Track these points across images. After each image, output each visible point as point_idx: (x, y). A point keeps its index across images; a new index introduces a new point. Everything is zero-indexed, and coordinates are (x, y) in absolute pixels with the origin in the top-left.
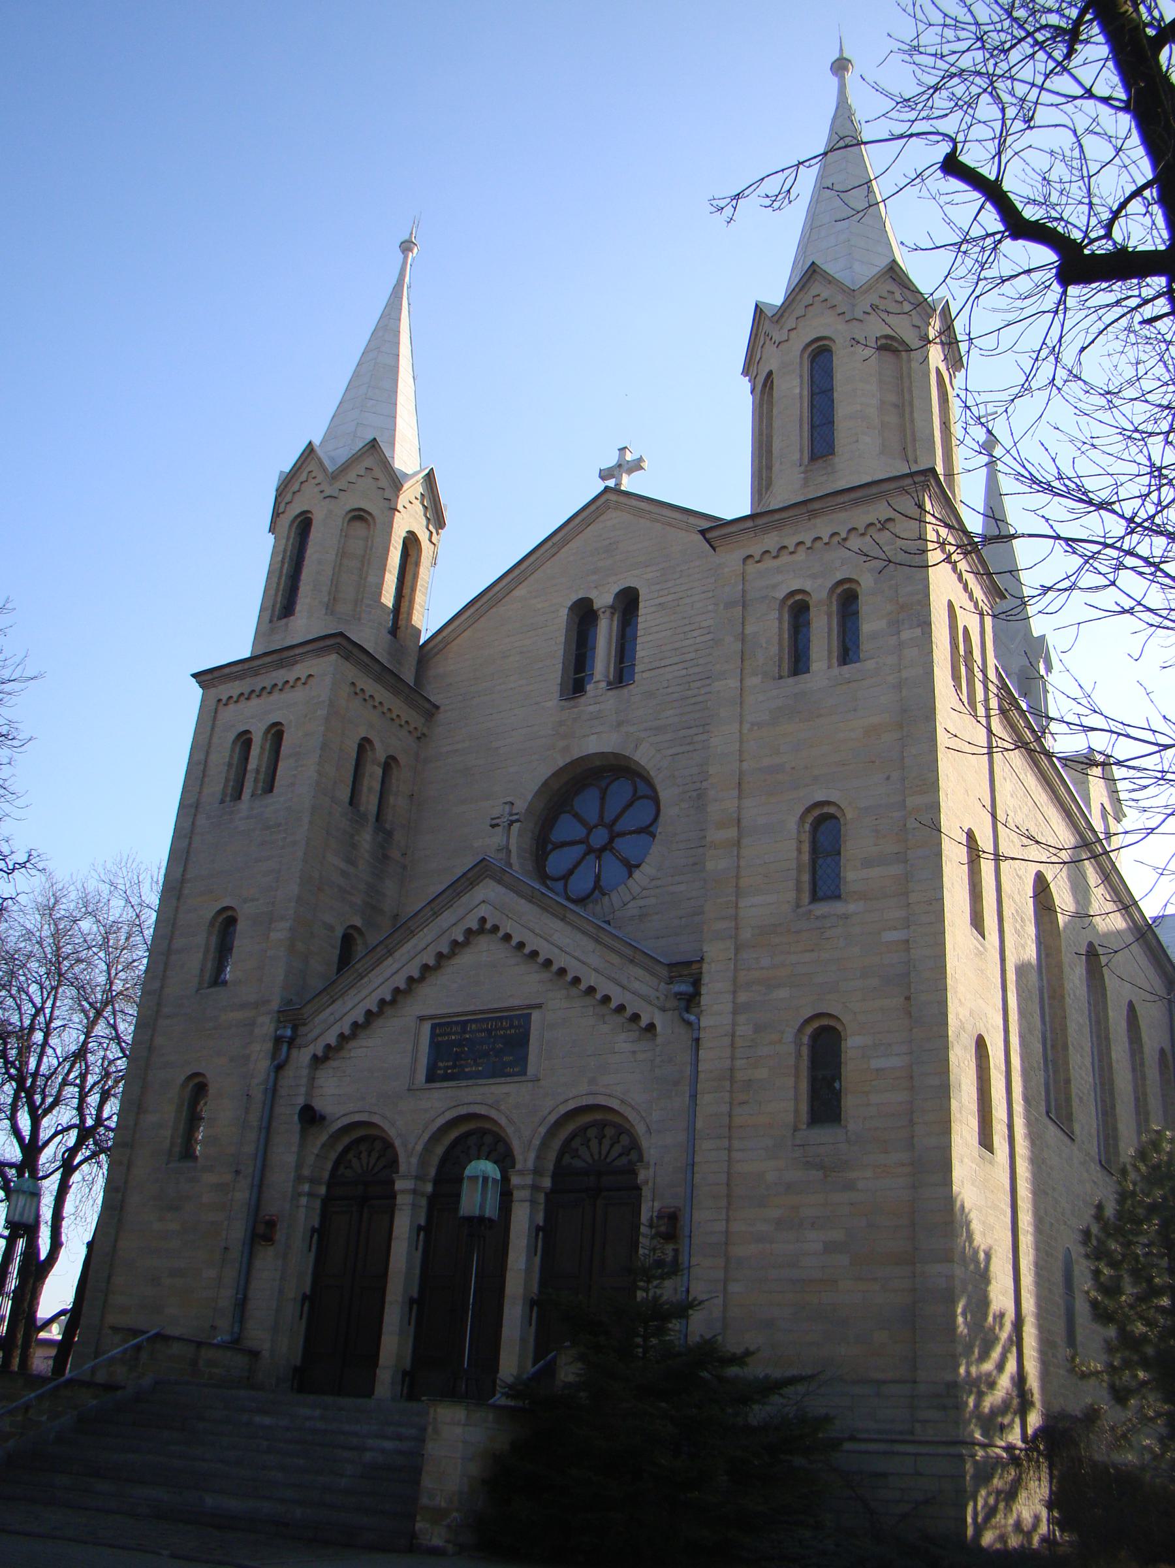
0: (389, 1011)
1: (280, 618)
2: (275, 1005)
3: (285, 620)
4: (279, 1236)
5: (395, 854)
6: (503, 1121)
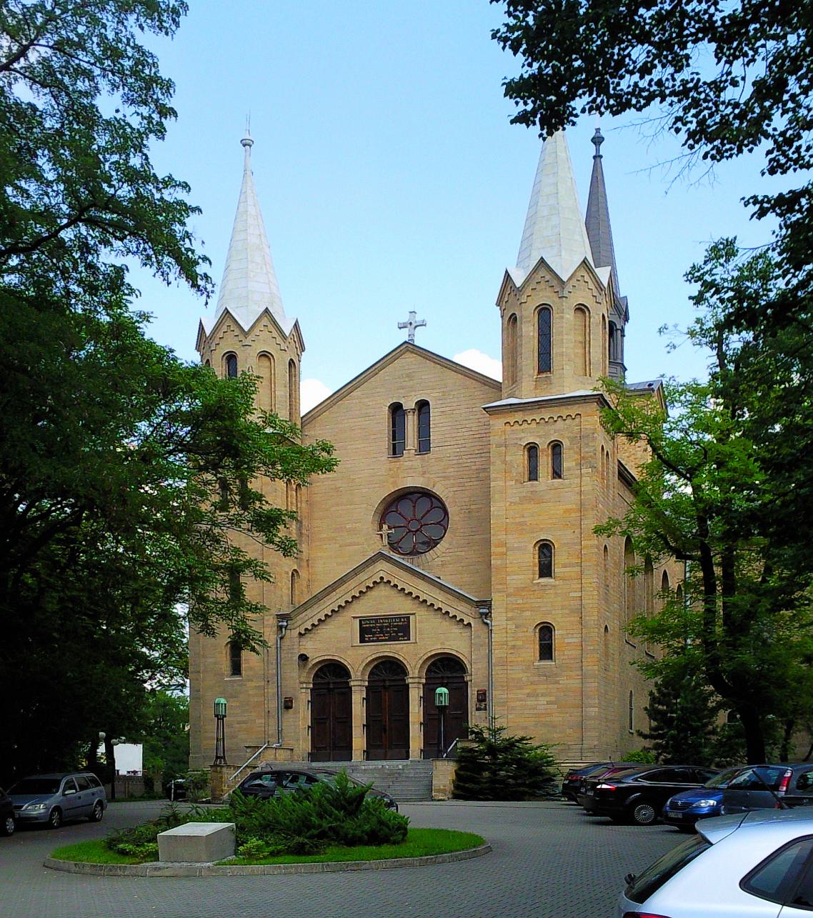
5: (304, 531)
6: (401, 659)
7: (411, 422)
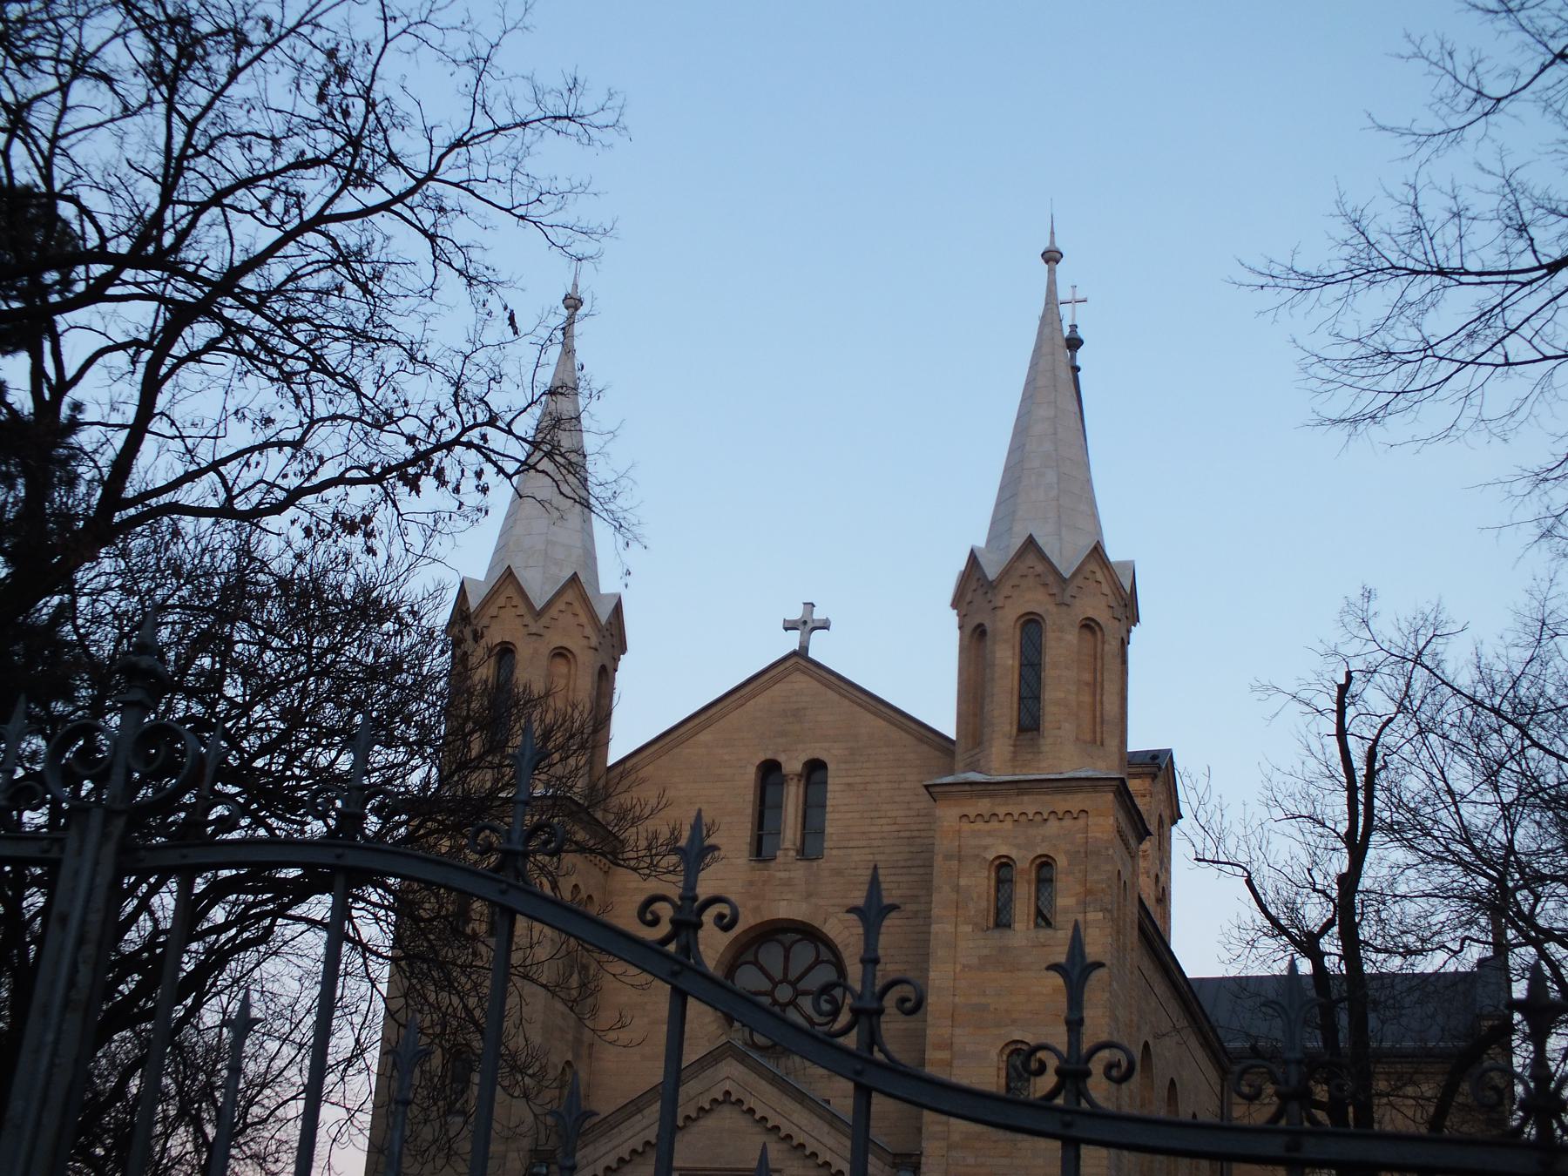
7: (793, 796)
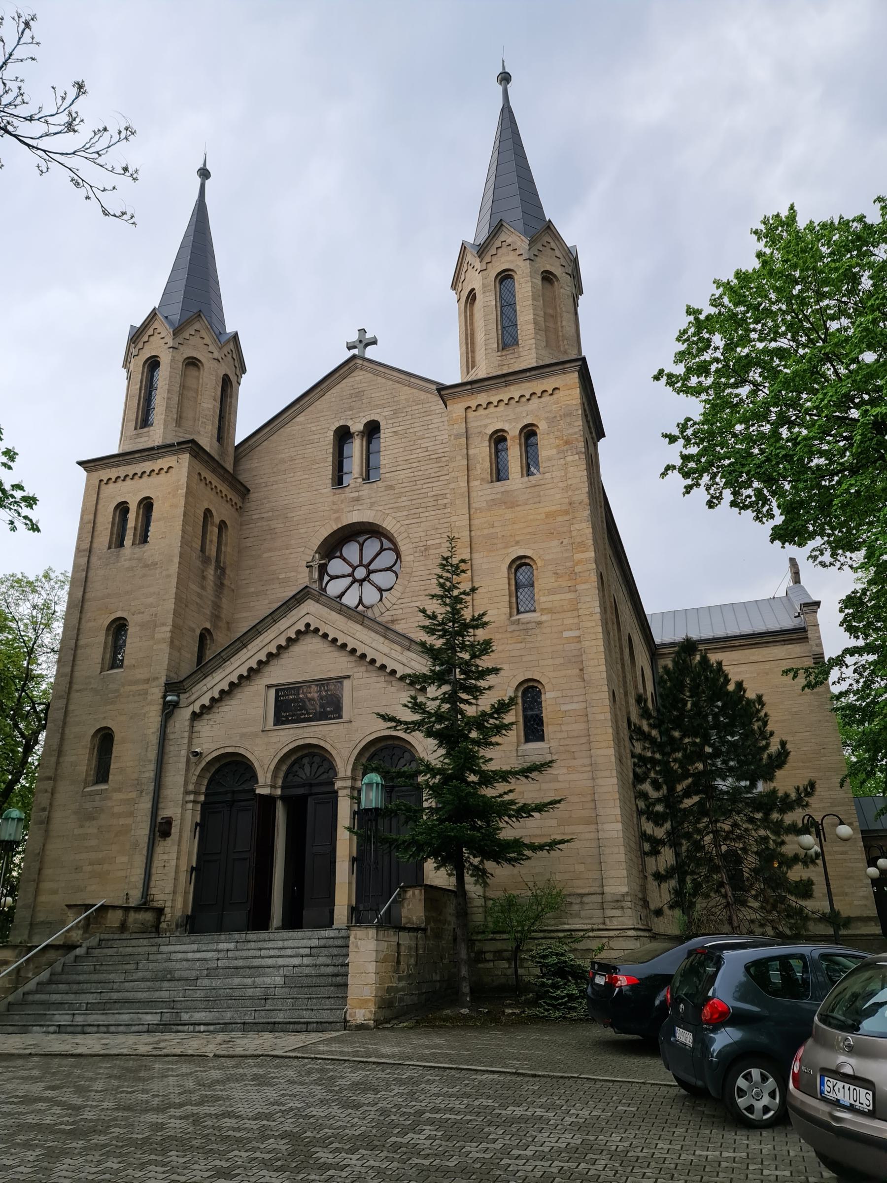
0: (244, 683)
1: (141, 428)
2: (163, 680)
3: (146, 430)
4: (175, 830)
6: (328, 747)
